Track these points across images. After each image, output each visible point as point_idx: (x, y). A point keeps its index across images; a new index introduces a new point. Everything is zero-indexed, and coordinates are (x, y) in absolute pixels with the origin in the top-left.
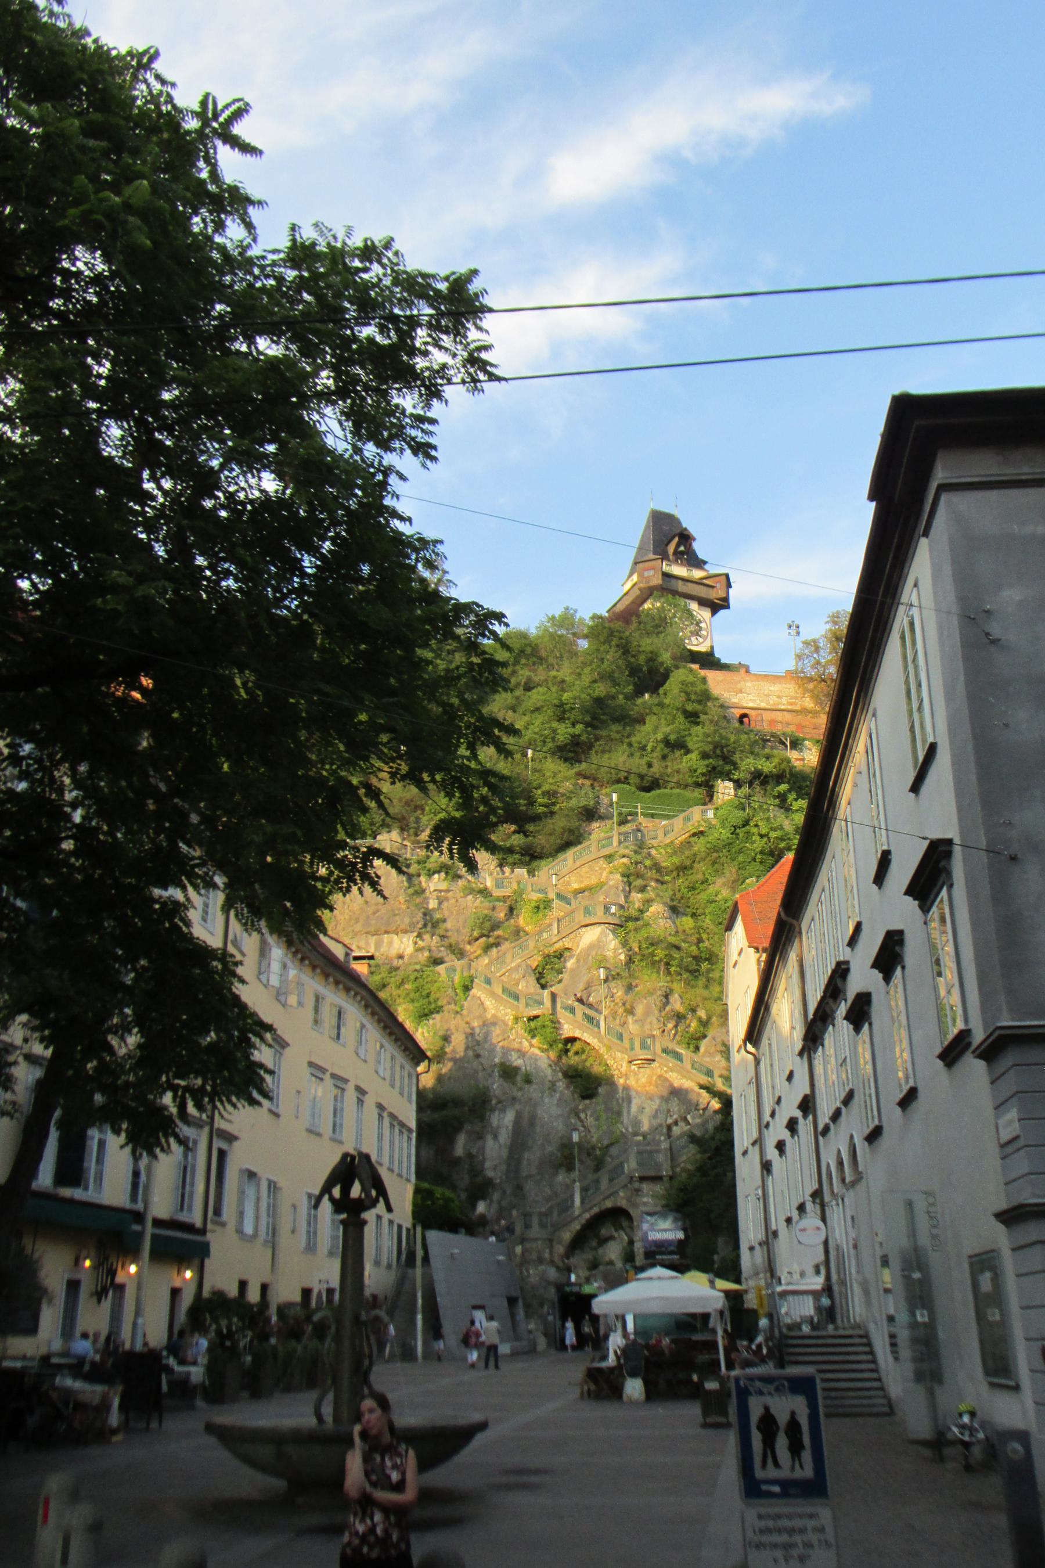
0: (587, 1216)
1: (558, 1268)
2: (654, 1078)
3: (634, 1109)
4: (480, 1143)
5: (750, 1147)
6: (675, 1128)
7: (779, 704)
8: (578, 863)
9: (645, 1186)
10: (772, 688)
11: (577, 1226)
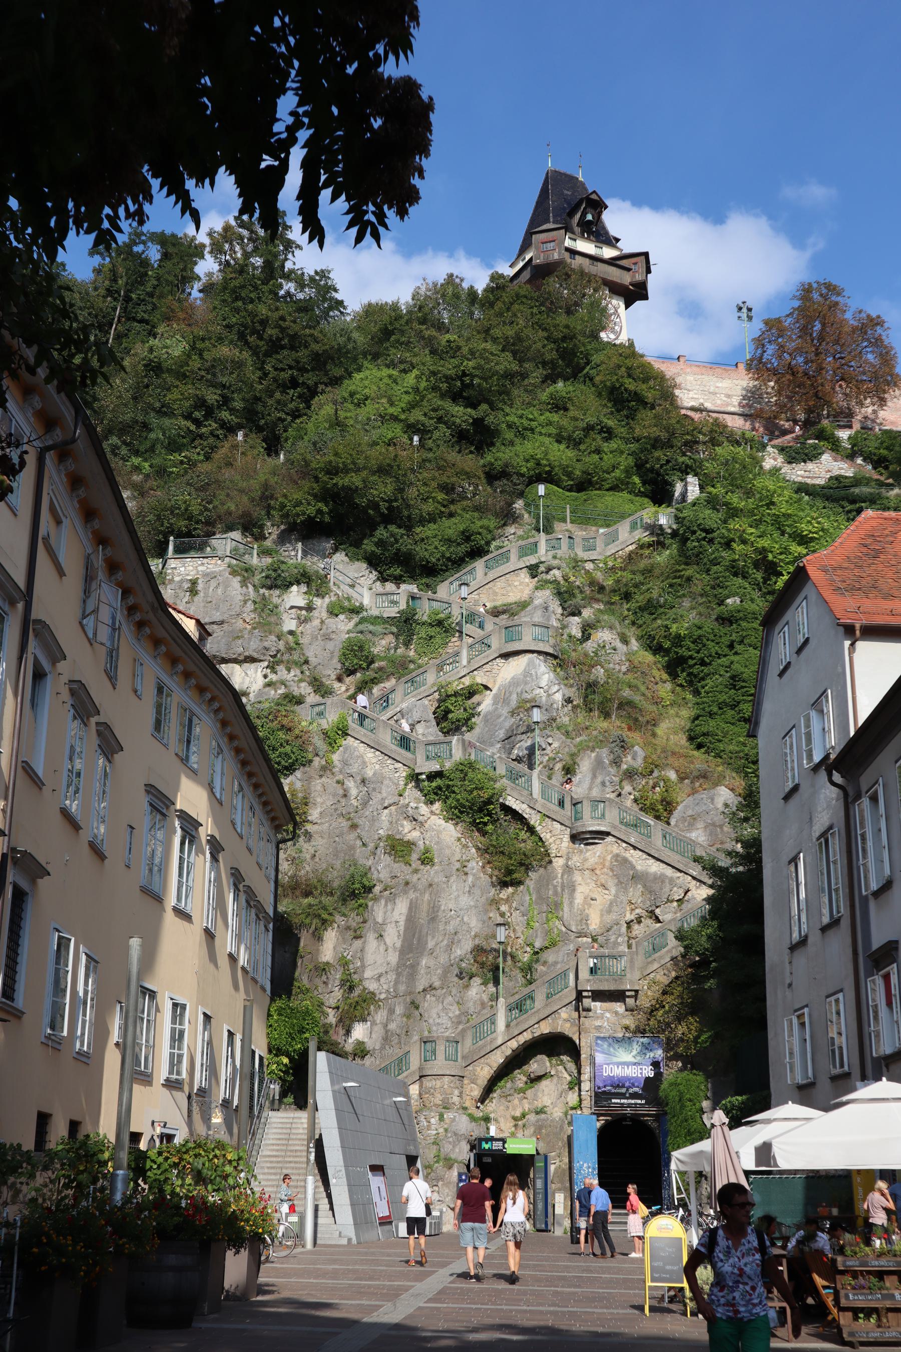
0: (514, 1044)
1: (472, 1118)
2: (609, 858)
3: (579, 899)
4: (358, 943)
5: (815, 938)
6: (636, 927)
7: (728, 405)
8: (492, 575)
9: (597, 1006)
10: (720, 385)
11: (498, 1059)
